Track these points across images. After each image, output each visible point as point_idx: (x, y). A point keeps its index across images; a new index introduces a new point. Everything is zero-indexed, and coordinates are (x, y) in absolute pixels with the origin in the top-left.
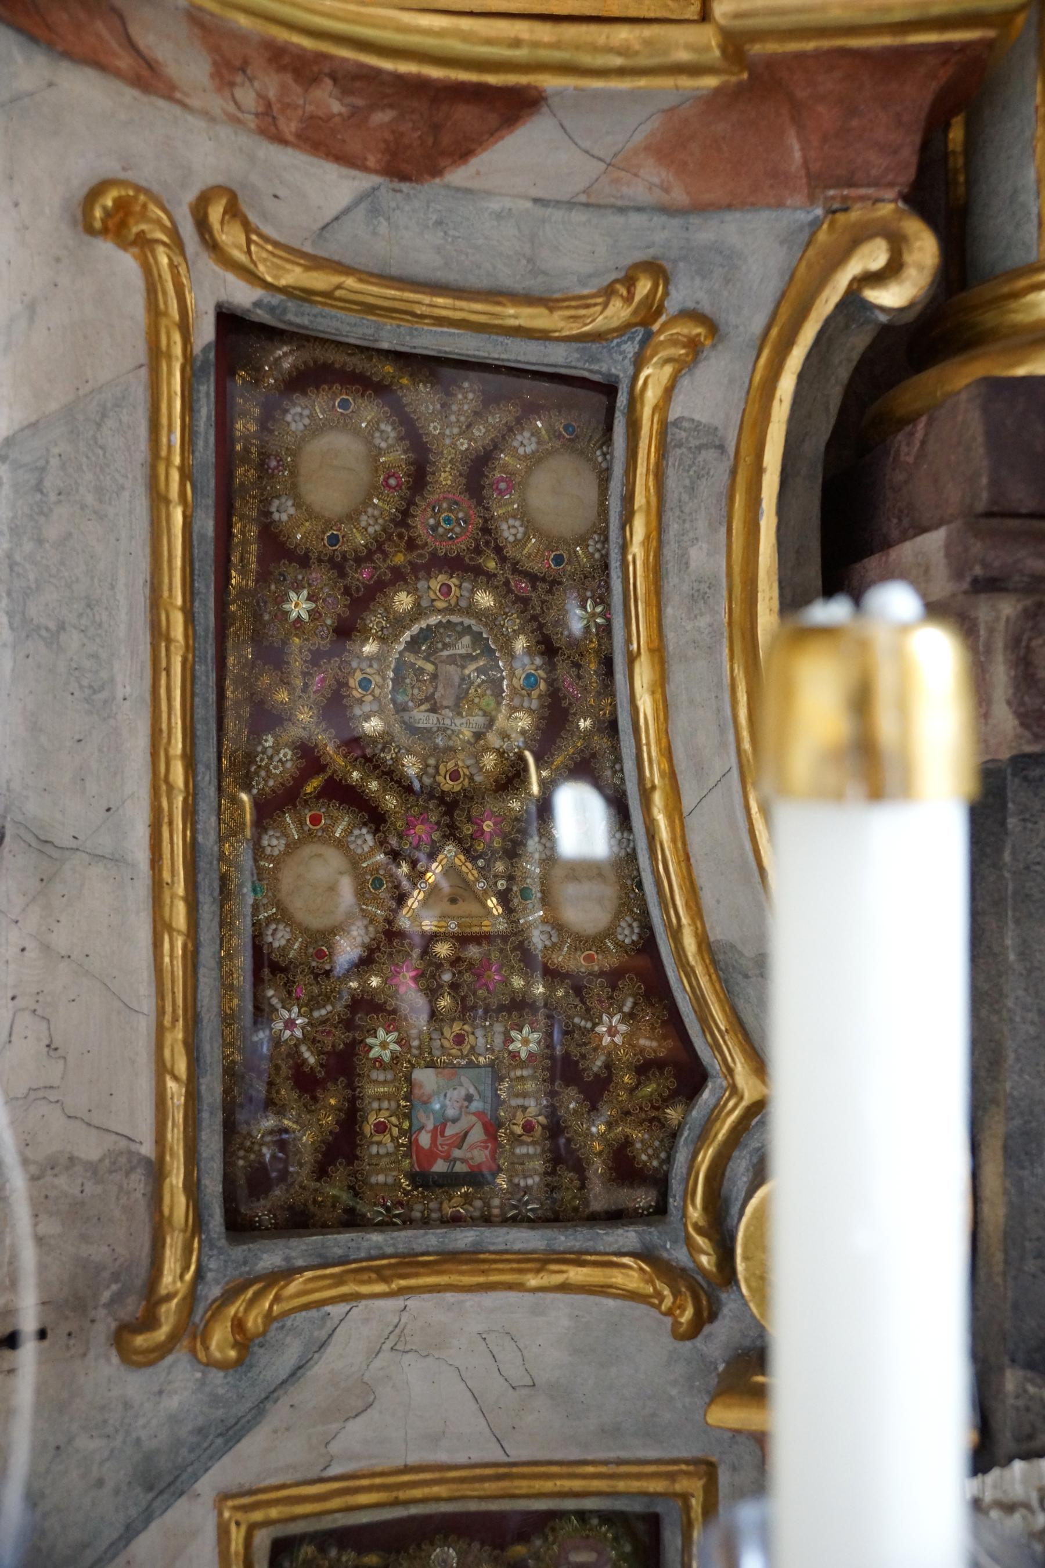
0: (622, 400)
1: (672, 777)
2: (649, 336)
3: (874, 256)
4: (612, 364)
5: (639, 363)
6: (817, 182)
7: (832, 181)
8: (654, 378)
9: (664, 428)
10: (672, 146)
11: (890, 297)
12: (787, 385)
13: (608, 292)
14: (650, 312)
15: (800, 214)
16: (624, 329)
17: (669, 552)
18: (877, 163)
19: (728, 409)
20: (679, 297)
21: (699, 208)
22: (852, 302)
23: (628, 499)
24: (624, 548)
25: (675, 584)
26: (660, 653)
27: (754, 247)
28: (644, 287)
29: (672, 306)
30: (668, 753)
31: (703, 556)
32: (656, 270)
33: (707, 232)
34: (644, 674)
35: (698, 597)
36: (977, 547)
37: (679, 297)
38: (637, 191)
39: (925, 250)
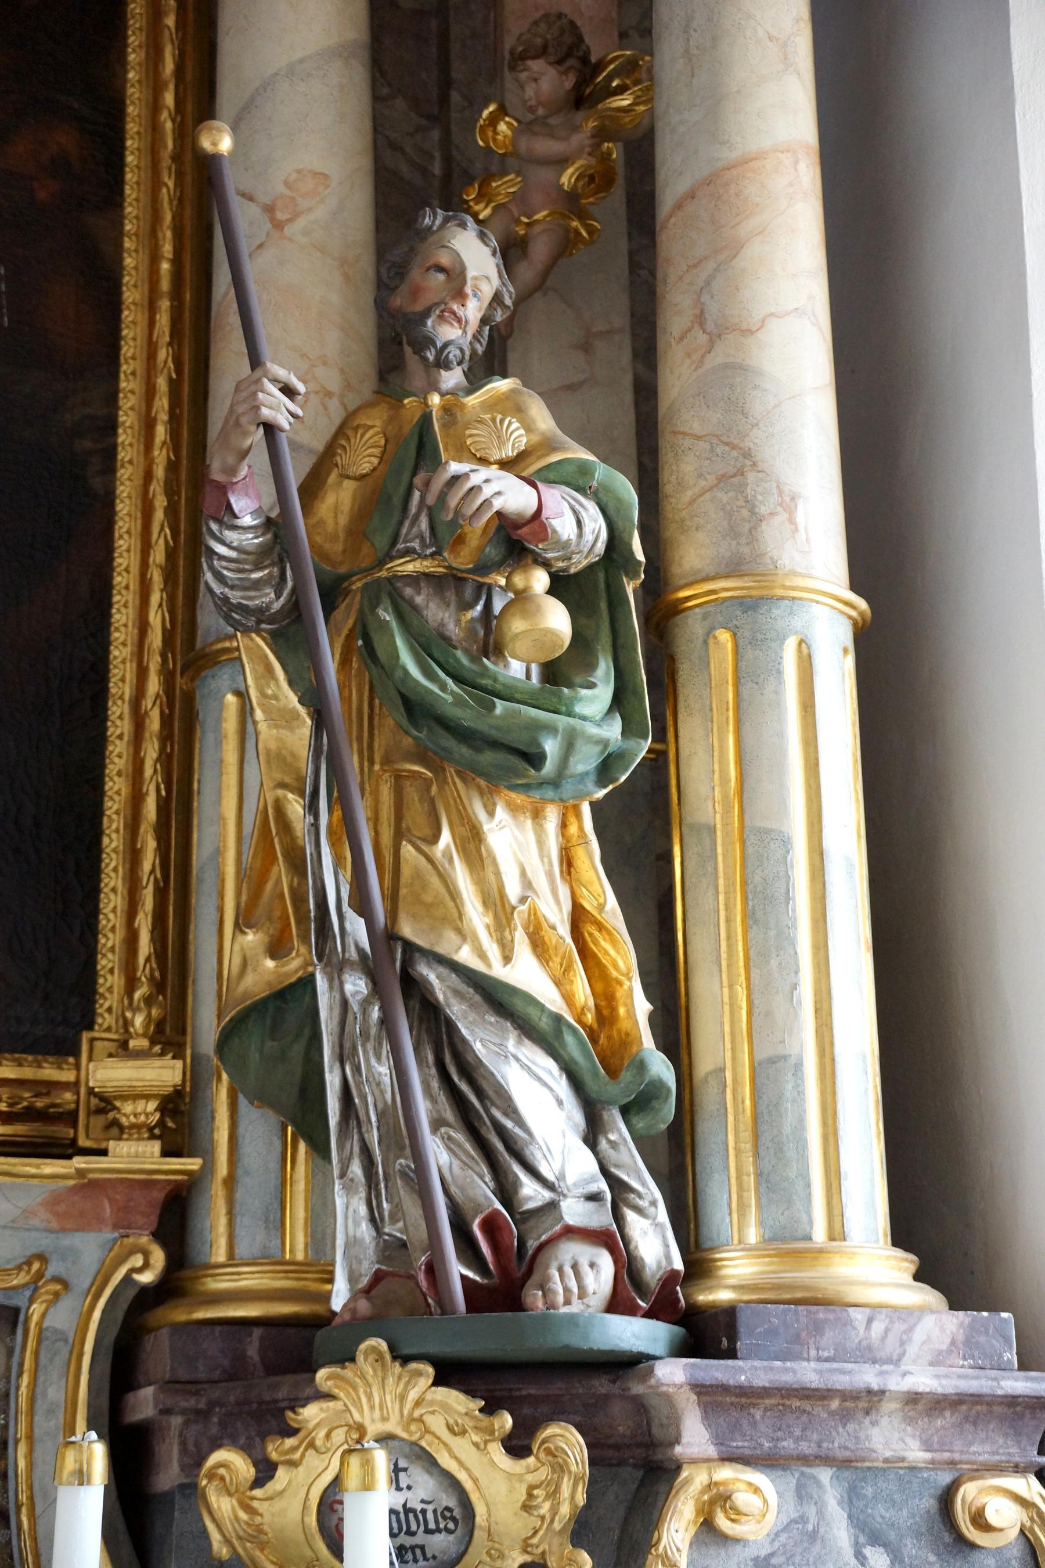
0: (22, 1317)
1: (31, 1498)
2: (36, 1289)
3: (138, 1261)
4: (20, 1301)
5: (31, 1301)
6: (116, 1227)
7: (123, 1224)
8: (37, 1309)
9: (41, 1330)
10: (54, 1202)
11: (146, 1278)
12: (97, 1315)
13: (19, 1268)
14: (40, 1275)
15: (109, 1235)
16: (25, 1286)
17: (39, 1390)
18: (140, 1220)
19: (72, 1323)
20: (52, 1270)
21: (63, 1230)
22: (127, 1279)
23: (21, 1365)
24: (18, 1388)
25: (41, 1406)
26: (30, 1438)
27: (89, 1247)
28: (36, 1266)
29: (48, 1275)
30: (30, 1487)
31: (54, 1392)
32: (42, 1258)
33: (68, 1240)
34: (22, 1449)
35: (51, 1412)
36: (162, 1396)
37: (52, 1270)
38: (35, 1222)
39: (159, 1257)
